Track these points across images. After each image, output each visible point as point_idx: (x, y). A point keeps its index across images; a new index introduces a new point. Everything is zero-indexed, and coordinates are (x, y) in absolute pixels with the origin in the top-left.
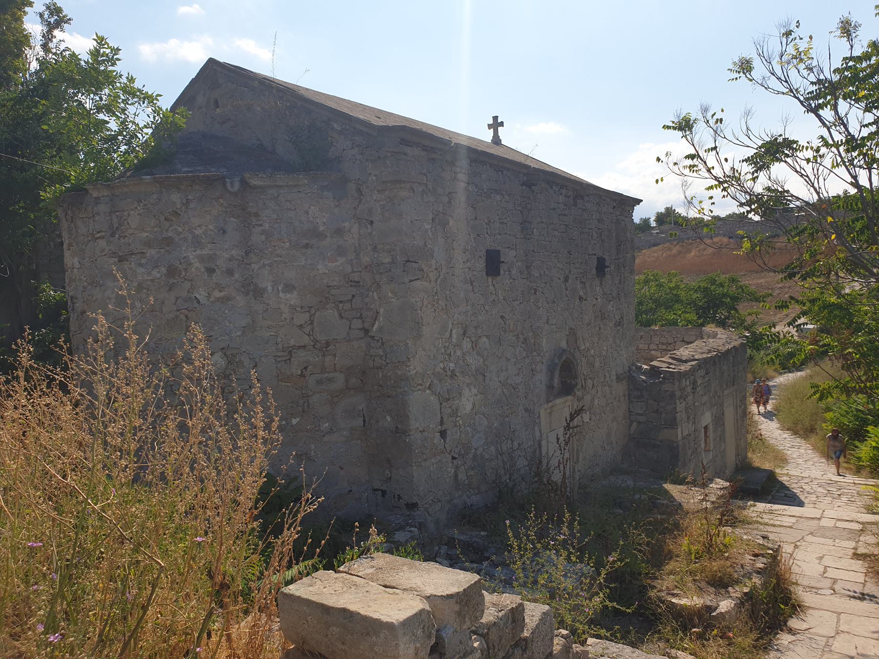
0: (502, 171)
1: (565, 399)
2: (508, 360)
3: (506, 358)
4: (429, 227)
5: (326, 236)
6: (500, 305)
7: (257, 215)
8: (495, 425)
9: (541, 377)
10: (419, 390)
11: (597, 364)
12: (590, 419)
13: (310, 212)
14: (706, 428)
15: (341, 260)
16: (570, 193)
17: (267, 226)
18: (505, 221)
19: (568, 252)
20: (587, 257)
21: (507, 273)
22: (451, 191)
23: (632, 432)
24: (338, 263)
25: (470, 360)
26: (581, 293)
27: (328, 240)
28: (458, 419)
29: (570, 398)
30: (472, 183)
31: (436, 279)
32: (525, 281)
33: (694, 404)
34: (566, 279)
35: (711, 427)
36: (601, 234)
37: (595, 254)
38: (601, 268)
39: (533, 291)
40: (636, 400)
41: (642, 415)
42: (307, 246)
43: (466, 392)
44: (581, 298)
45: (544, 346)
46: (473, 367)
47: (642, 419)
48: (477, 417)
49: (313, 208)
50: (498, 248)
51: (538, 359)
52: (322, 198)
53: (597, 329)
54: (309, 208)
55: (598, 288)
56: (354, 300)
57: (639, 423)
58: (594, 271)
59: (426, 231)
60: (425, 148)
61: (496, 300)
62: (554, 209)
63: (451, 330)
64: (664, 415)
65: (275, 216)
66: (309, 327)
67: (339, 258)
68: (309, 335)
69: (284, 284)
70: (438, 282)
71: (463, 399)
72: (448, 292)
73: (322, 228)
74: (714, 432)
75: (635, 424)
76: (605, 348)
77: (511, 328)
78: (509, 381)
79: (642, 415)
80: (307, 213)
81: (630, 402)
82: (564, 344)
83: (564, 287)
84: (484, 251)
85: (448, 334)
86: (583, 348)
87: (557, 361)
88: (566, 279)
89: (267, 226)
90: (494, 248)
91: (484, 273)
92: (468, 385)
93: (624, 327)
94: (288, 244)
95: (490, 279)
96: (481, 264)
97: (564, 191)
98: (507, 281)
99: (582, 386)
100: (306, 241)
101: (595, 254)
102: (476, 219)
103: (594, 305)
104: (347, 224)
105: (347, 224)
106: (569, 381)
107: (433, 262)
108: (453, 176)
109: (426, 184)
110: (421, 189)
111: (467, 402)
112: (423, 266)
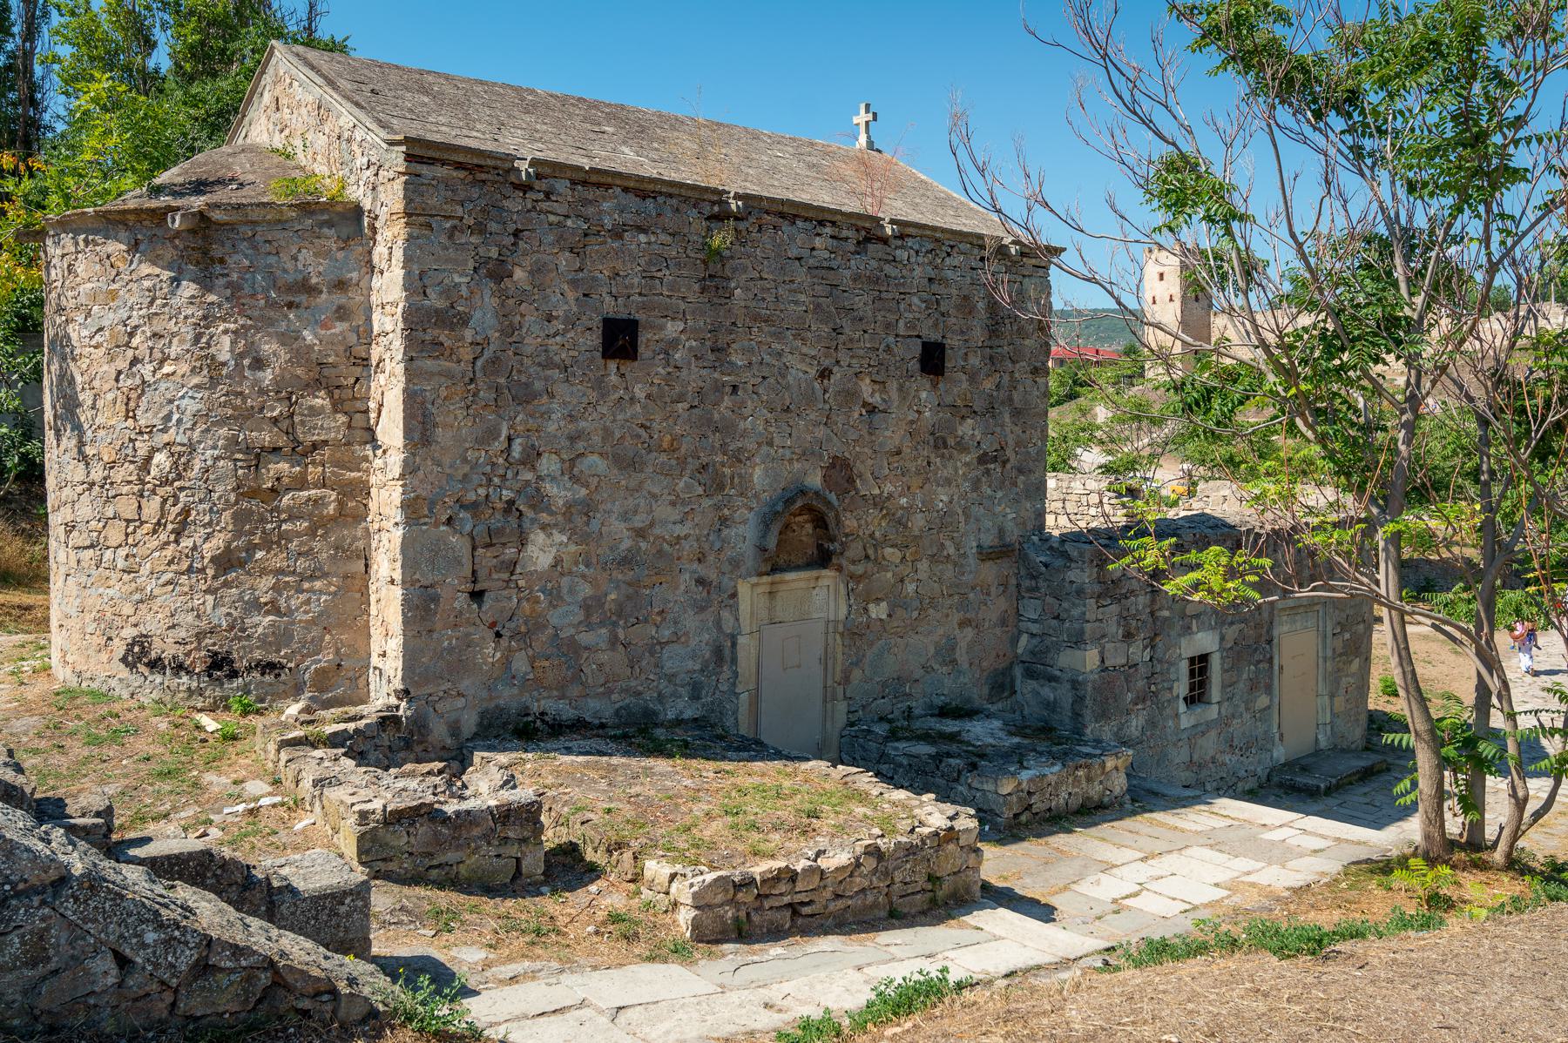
0: (655, 198)
1: (814, 573)
2: (654, 496)
3: (649, 492)
4: (468, 279)
5: (321, 292)
6: (638, 408)
7: (222, 261)
8: (613, 596)
9: (744, 534)
10: (425, 524)
11: (918, 522)
12: (890, 616)
13: (300, 258)
14: (1200, 664)
15: (340, 327)
16: (845, 233)
17: (235, 276)
18: (659, 274)
19: (834, 330)
20: (891, 339)
21: (662, 356)
22: (520, 227)
23: (1020, 651)
24: (336, 330)
25: (550, 488)
26: (876, 399)
27: (324, 296)
28: (514, 578)
29: (825, 572)
30: (577, 216)
31: (475, 359)
32: (704, 372)
33: (1152, 613)
34: (825, 374)
35: (1216, 664)
36: (938, 302)
37: (919, 337)
38: (933, 360)
39: (728, 389)
40: (1027, 595)
41: (1035, 621)
42: (290, 305)
43: (539, 537)
44: (872, 410)
45: (755, 481)
46: (561, 502)
47: (1035, 628)
48: (565, 581)
49: (304, 251)
50: (640, 316)
51: (739, 501)
52: (319, 238)
53: (921, 462)
54: (299, 251)
55: (924, 395)
56: (357, 386)
57: (1033, 635)
58: (914, 365)
59: (457, 285)
60: (459, 166)
61: (627, 397)
62: (799, 259)
63: (510, 439)
64: (1067, 624)
65: (247, 263)
66: (288, 421)
67: (338, 324)
68: (287, 433)
69: (254, 358)
70: (479, 363)
71: (530, 548)
72: (502, 381)
73: (314, 281)
74: (1225, 671)
75: (1024, 639)
76: (945, 498)
77: (665, 445)
78: (657, 531)
79: (1035, 621)
80: (295, 259)
81: (1020, 597)
82: (815, 480)
83: (817, 385)
84: (596, 322)
85: (499, 444)
86: (877, 491)
87: (779, 508)
88: (825, 374)
89: (235, 276)
90: (625, 316)
91: (599, 355)
92: (544, 527)
93: (1008, 466)
94: (263, 302)
95: (612, 365)
96: (594, 340)
97: (828, 230)
98: (660, 369)
99: (867, 557)
100: (291, 298)
101: (919, 337)
102: (581, 269)
103: (912, 422)
104: (355, 275)
105: (355, 275)
106: (826, 545)
107: (468, 334)
108: (529, 206)
109: (461, 219)
110: (448, 225)
111: (541, 552)
112: (442, 338)
